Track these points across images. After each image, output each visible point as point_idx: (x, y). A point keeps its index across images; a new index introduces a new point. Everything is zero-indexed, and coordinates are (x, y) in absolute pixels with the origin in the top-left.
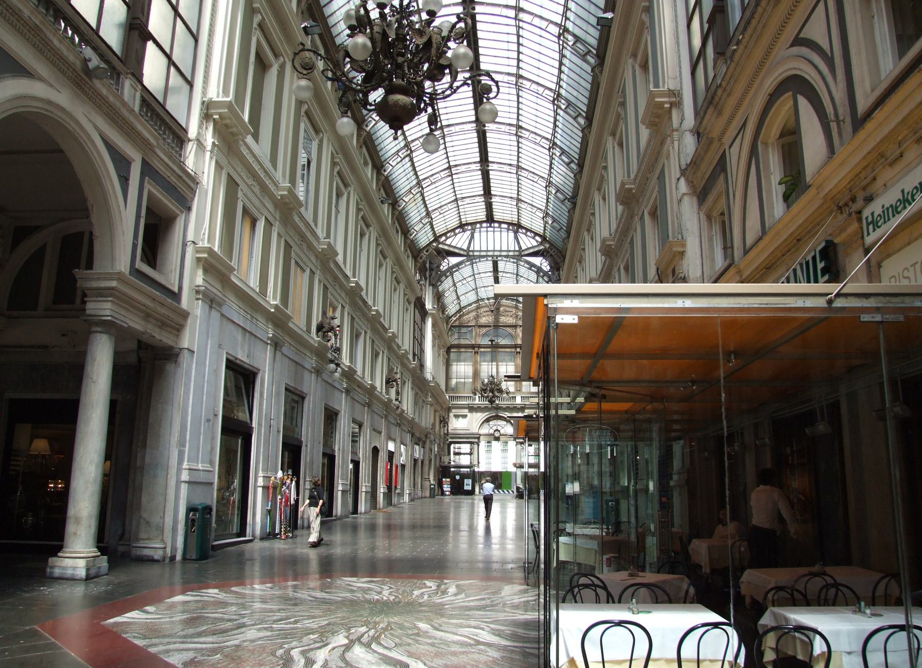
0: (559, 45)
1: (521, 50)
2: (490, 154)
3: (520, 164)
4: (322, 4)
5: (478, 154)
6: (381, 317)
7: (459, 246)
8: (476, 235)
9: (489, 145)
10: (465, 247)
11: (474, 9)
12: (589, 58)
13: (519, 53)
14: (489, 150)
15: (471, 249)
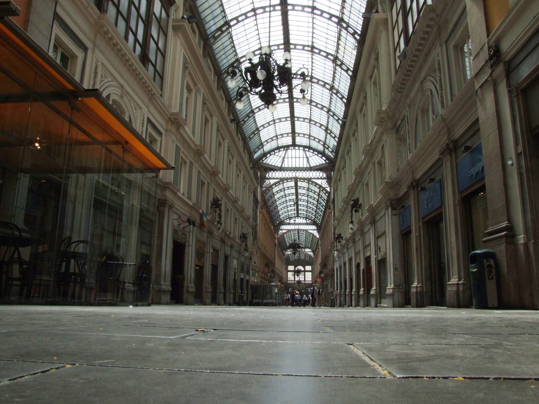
0: (338, 28)
1: (314, 22)
2: (295, 113)
3: (312, 99)
4: (198, 6)
5: (289, 113)
6: (219, 173)
7: (276, 165)
8: (286, 160)
9: (295, 109)
10: (280, 166)
11: (287, 7)
12: (356, 36)
13: (313, 23)
14: (295, 111)
15: (283, 166)
